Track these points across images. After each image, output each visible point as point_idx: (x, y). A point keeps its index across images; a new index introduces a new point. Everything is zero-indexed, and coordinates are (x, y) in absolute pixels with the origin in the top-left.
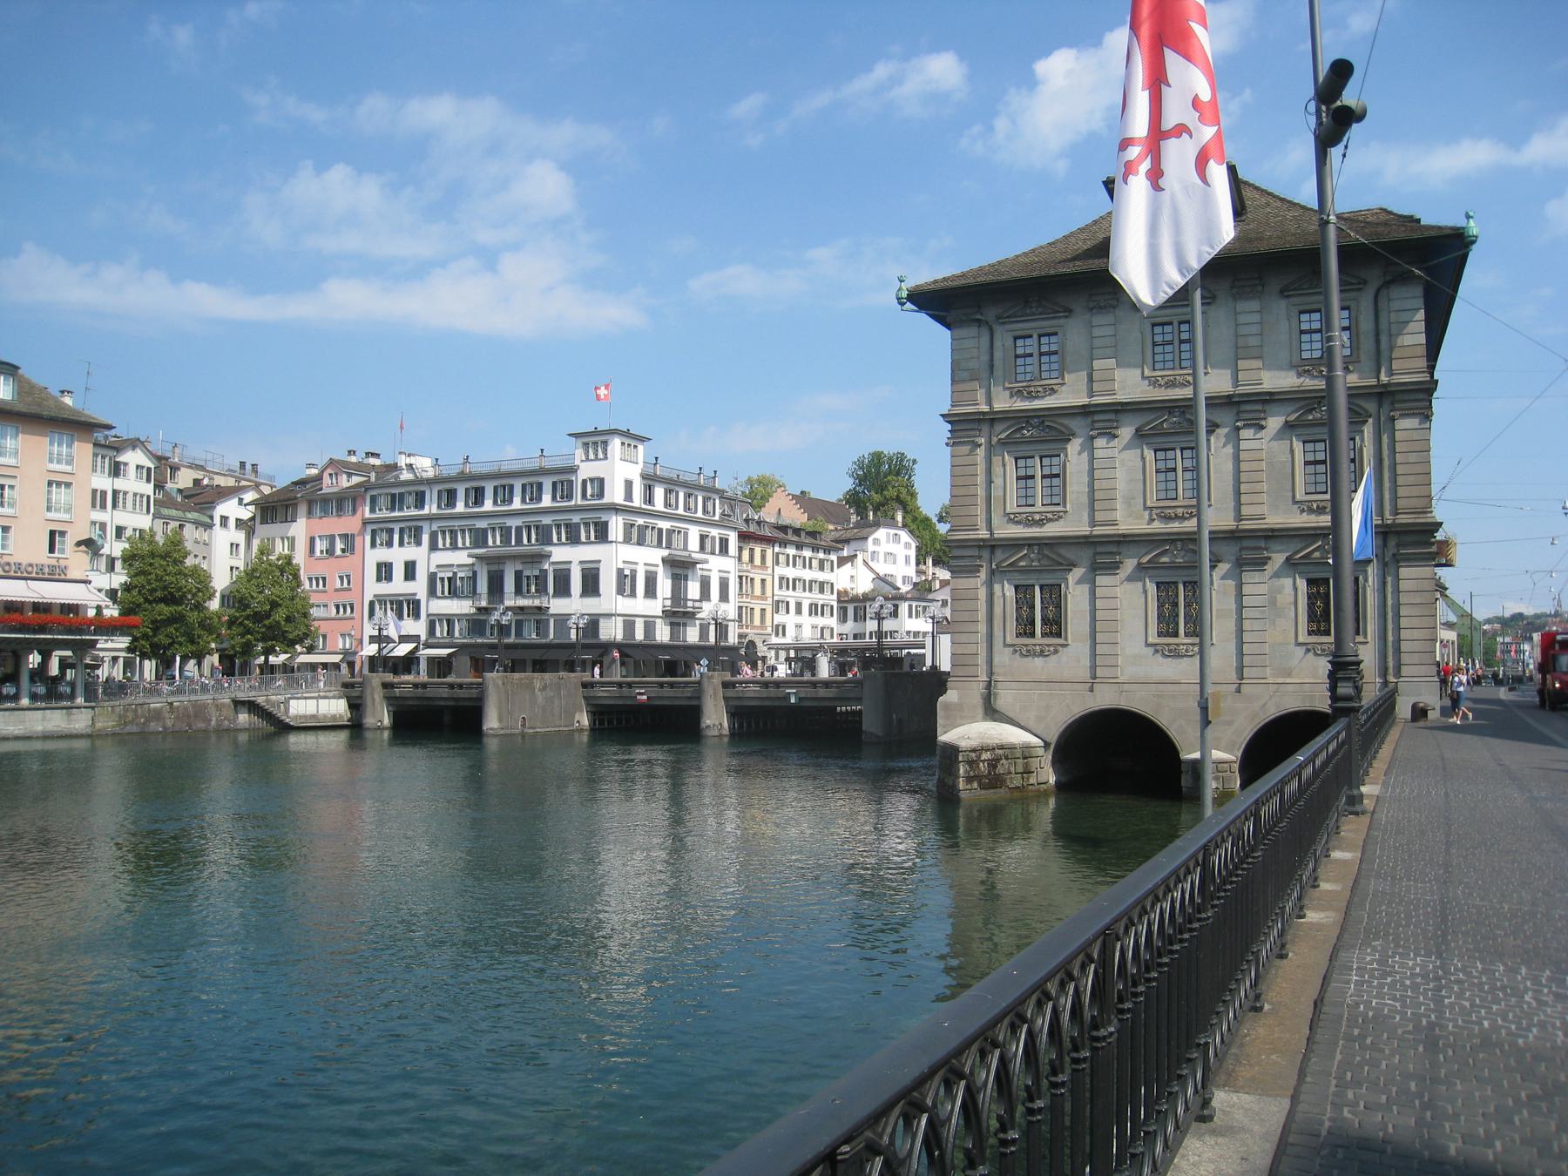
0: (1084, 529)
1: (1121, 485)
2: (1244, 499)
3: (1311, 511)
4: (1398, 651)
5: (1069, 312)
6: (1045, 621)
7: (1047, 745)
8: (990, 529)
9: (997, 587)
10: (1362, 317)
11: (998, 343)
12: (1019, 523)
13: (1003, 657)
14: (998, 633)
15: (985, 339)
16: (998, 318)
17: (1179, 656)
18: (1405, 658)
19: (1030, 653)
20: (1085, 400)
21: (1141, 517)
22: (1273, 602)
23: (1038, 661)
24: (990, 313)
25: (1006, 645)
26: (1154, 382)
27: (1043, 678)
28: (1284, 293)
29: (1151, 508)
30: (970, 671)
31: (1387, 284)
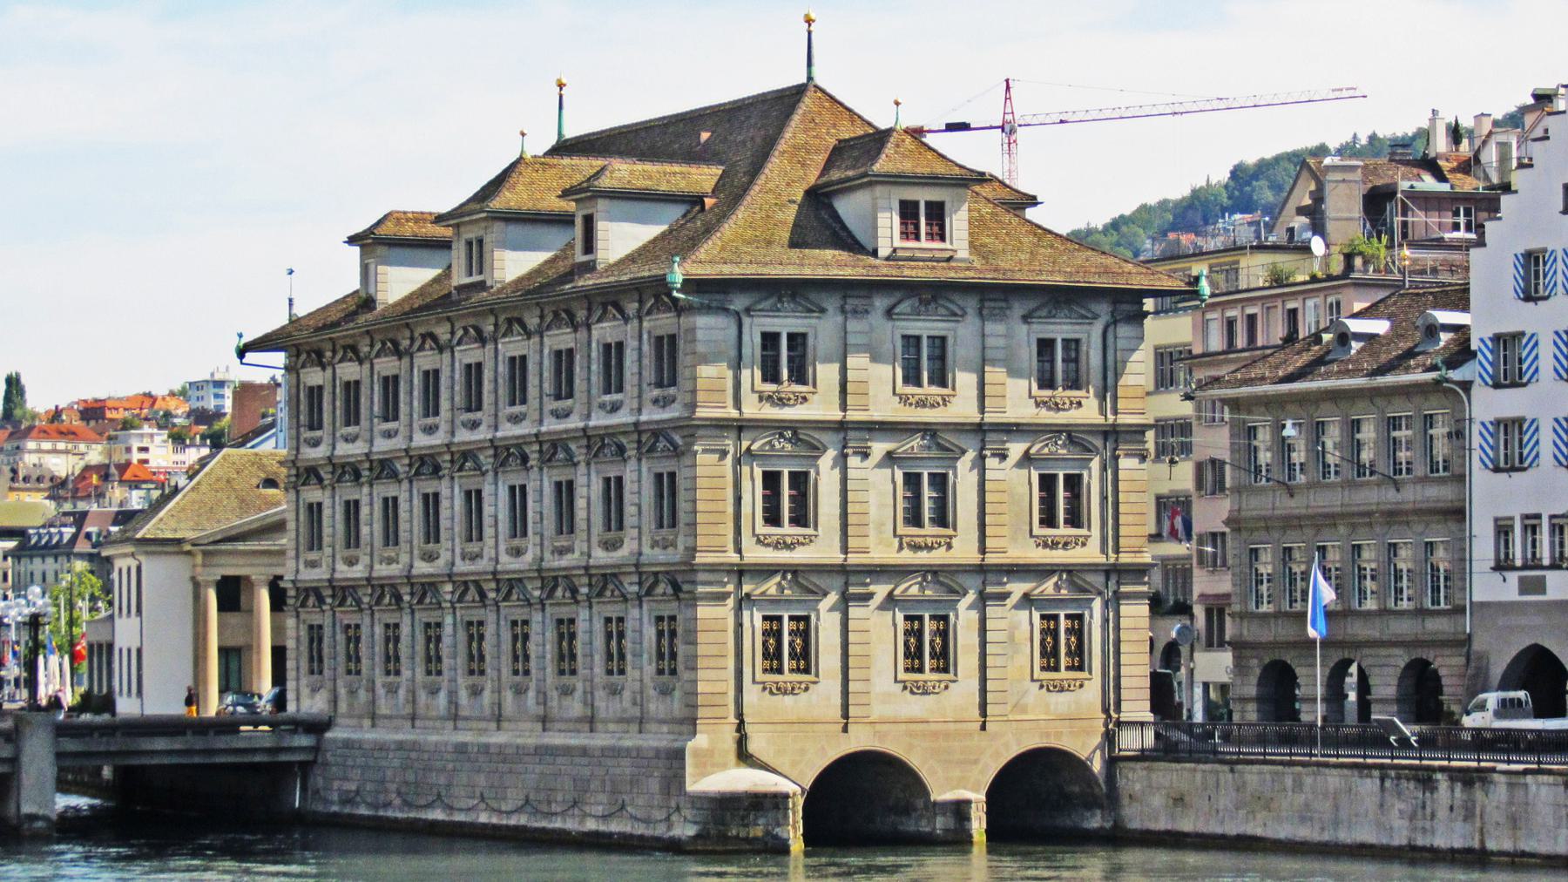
0: (836, 557)
1: (873, 511)
2: (989, 531)
3: (1046, 545)
4: (1118, 687)
5: (823, 311)
6: (793, 655)
7: (803, 790)
8: (739, 551)
9: (746, 614)
10: (1092, 352)
11: (746, 338)
12: (768, 545)
13: (751, 694)
14: (747, 670)
15: (733, 331)
16: (748, 310)
17: (925, 693)
18: (1124, 694)
19: (782, 691)
20: (837, 415)
21: (890, 545)
22: (1012, 638)
23: (788, 699)
24: (739, 302)
25: (754, 682)
26: (904, 399)
27: (794, 719)
28: (1026, 319)
29: (901, 537)
30: (718, 712)
31: (1115, 322)
